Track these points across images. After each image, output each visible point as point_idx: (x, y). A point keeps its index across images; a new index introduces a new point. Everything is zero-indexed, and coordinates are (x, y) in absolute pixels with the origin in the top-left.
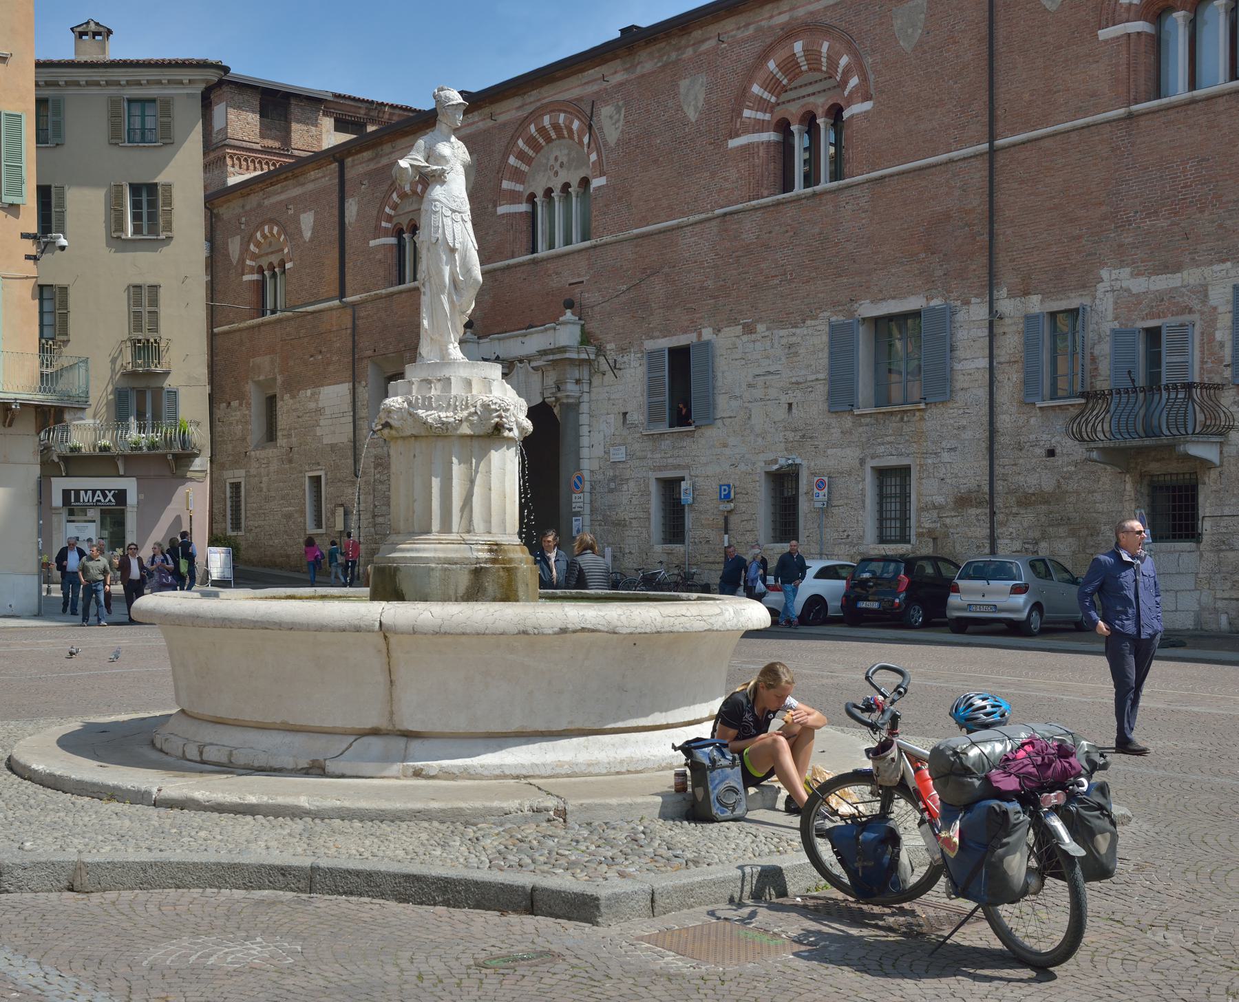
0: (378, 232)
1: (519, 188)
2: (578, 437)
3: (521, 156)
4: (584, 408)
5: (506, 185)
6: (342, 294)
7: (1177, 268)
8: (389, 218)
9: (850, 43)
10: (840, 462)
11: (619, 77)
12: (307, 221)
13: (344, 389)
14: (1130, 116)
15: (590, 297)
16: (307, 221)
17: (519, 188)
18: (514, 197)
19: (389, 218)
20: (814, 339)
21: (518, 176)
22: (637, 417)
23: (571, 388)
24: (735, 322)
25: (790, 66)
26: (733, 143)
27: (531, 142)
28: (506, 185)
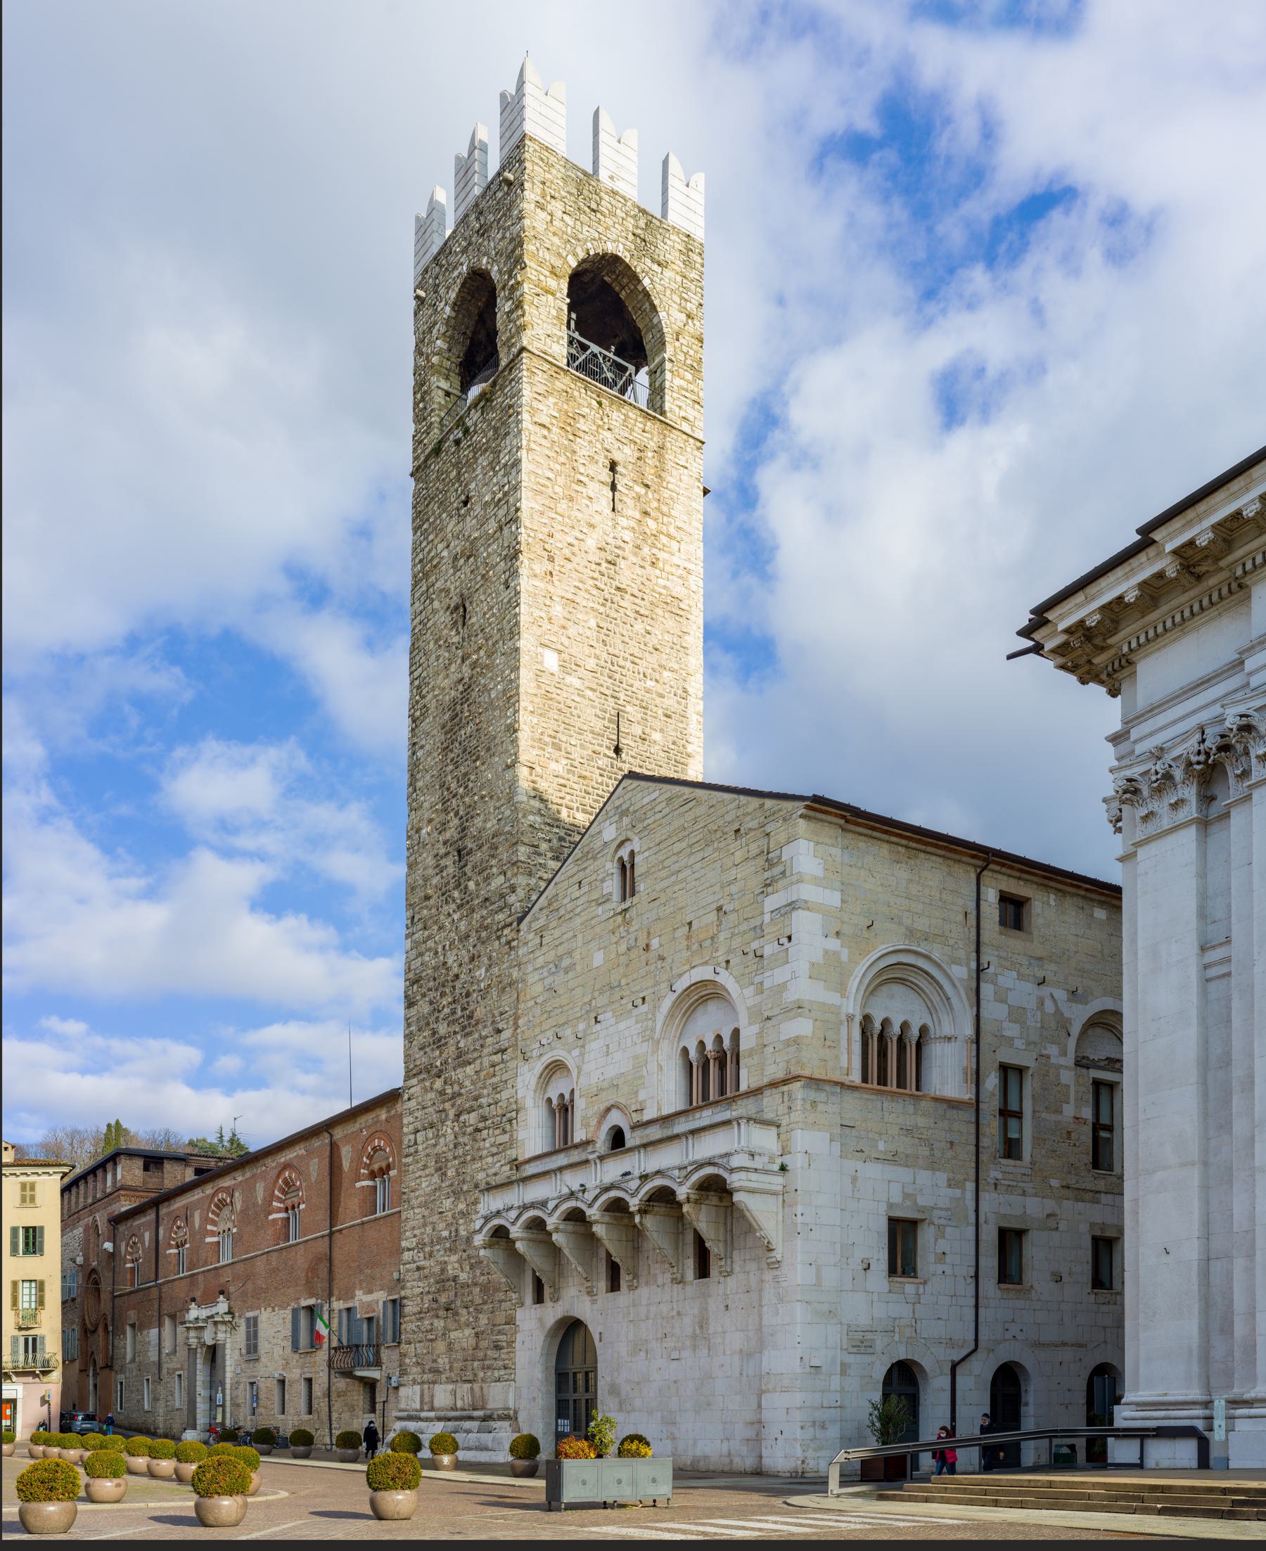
0: (170, 1247)
1: (215, 1229)
2: (224, 1360)
3: (213, 1213)
4: (228, 1346)
5: (209, 1227)
6: (157, 1279)
7: (370, 1292)
8: (174, 1239)
9: (299, 1173)
10: (294, 1375)
11: (240, 1179)
12: (147, 1236)
13: (156, 1330)
14: (363, 1223)
15: (232, 1289)
16: (147, 1236)
17: (215, 1229)
18: (213, 1234)
19: (174, 1239)
20: (287, 1314)
21: (214, 1223)
22: (244, 1351)
23: (221, 1336)
24: (269, 1305)
25: (286, 1182)
26: (271, 1217)
27: (216, 1206)
28: (209, 1227)
